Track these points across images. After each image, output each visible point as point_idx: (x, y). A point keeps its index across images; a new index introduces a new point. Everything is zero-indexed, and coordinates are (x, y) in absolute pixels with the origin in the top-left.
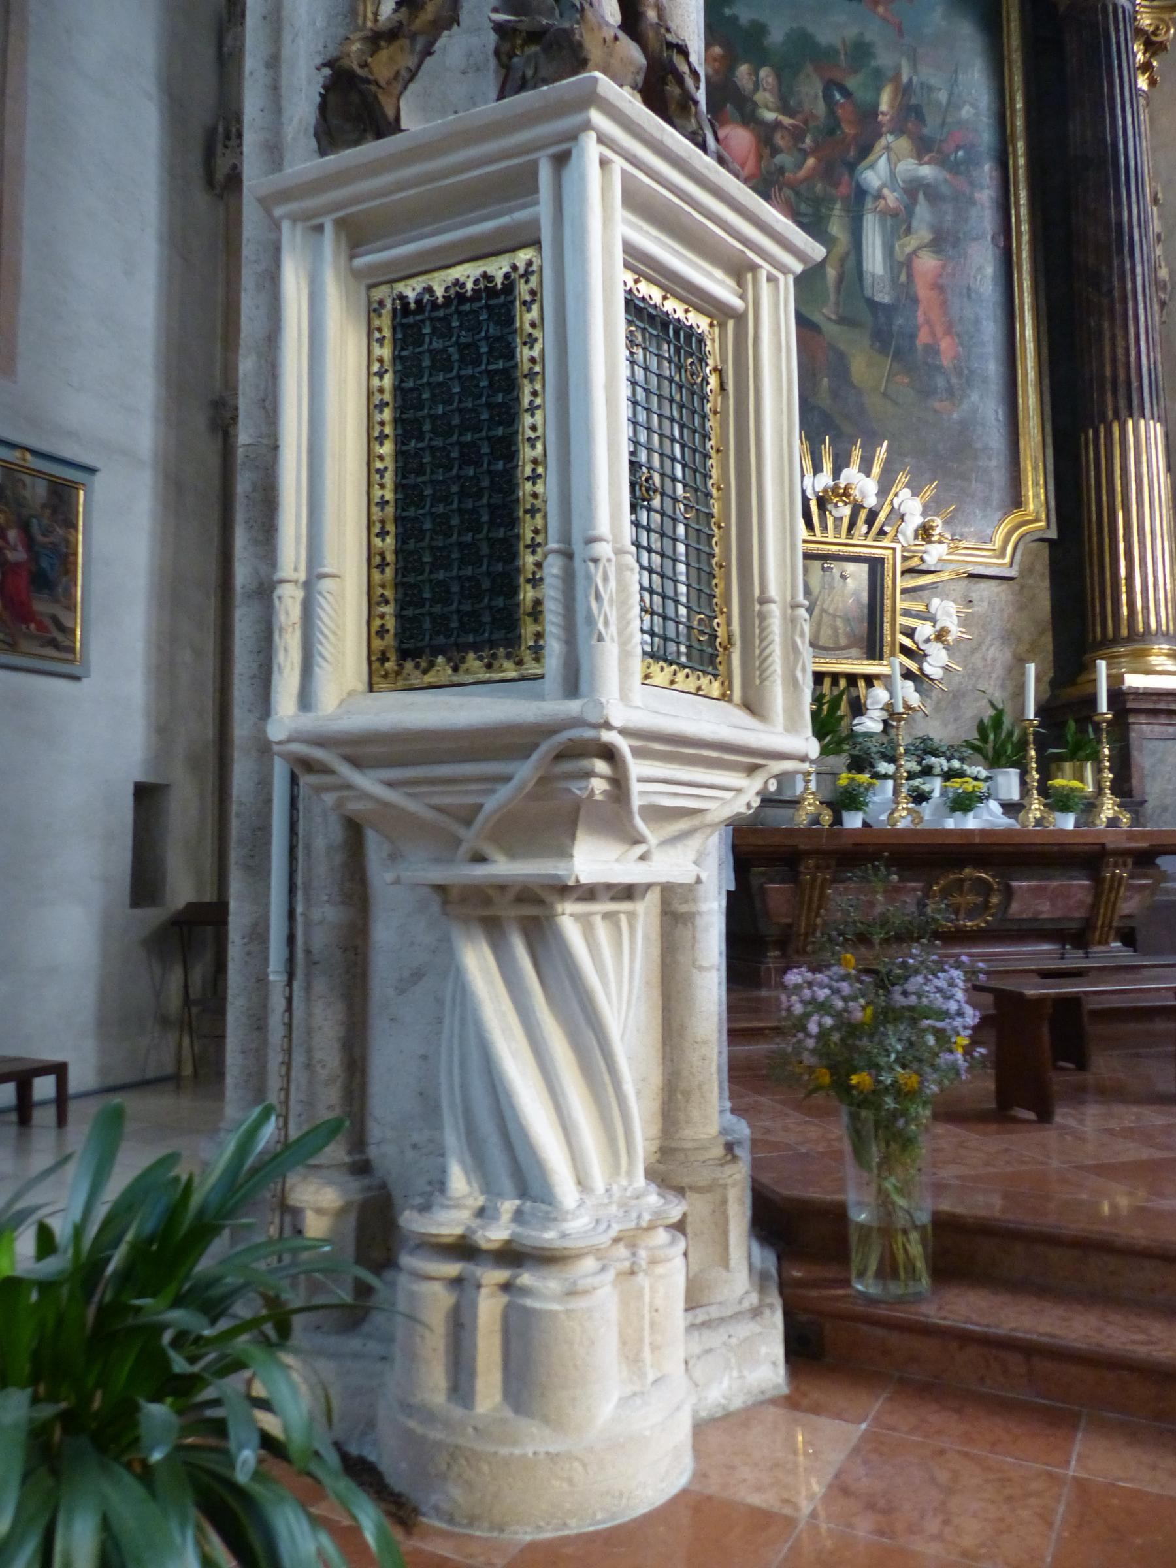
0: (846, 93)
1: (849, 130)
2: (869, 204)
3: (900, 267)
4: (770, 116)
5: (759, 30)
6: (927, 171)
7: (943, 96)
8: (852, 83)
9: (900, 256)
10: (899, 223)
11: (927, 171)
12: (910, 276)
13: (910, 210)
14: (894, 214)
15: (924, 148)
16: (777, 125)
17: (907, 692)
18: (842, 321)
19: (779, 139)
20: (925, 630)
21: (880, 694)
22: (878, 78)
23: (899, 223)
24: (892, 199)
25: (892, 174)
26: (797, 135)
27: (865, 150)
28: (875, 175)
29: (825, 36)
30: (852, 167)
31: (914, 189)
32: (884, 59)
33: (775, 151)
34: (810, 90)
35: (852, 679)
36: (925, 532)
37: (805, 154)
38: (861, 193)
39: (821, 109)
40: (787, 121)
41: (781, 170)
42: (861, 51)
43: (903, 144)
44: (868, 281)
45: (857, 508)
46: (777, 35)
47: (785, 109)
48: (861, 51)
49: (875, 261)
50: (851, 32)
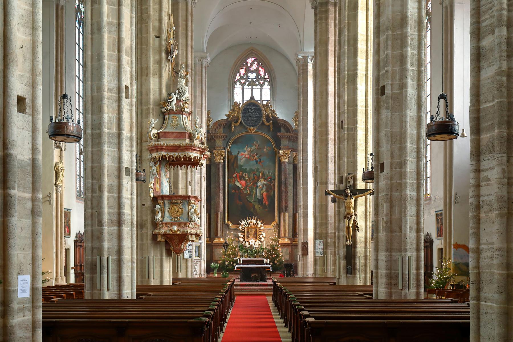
3: (262, 195)
5: (246, 169)
6: (265, 182)
8: (257, 173)
11: (265, 182)
15: (265, 180)
20: (261, 236)
22: (260, 172)
23: (262, 189)
24: (261, 186)
26: (250, 181)
28: (259, 184)
29: (253, 168)
30: (256, 183)
31: (264, 185)
32: (260, 170)
34: (252, 175)
36: (261, 226)
38: (257, 186)
43: (263, 179)
46: (248, 169)
49: (258, 194)
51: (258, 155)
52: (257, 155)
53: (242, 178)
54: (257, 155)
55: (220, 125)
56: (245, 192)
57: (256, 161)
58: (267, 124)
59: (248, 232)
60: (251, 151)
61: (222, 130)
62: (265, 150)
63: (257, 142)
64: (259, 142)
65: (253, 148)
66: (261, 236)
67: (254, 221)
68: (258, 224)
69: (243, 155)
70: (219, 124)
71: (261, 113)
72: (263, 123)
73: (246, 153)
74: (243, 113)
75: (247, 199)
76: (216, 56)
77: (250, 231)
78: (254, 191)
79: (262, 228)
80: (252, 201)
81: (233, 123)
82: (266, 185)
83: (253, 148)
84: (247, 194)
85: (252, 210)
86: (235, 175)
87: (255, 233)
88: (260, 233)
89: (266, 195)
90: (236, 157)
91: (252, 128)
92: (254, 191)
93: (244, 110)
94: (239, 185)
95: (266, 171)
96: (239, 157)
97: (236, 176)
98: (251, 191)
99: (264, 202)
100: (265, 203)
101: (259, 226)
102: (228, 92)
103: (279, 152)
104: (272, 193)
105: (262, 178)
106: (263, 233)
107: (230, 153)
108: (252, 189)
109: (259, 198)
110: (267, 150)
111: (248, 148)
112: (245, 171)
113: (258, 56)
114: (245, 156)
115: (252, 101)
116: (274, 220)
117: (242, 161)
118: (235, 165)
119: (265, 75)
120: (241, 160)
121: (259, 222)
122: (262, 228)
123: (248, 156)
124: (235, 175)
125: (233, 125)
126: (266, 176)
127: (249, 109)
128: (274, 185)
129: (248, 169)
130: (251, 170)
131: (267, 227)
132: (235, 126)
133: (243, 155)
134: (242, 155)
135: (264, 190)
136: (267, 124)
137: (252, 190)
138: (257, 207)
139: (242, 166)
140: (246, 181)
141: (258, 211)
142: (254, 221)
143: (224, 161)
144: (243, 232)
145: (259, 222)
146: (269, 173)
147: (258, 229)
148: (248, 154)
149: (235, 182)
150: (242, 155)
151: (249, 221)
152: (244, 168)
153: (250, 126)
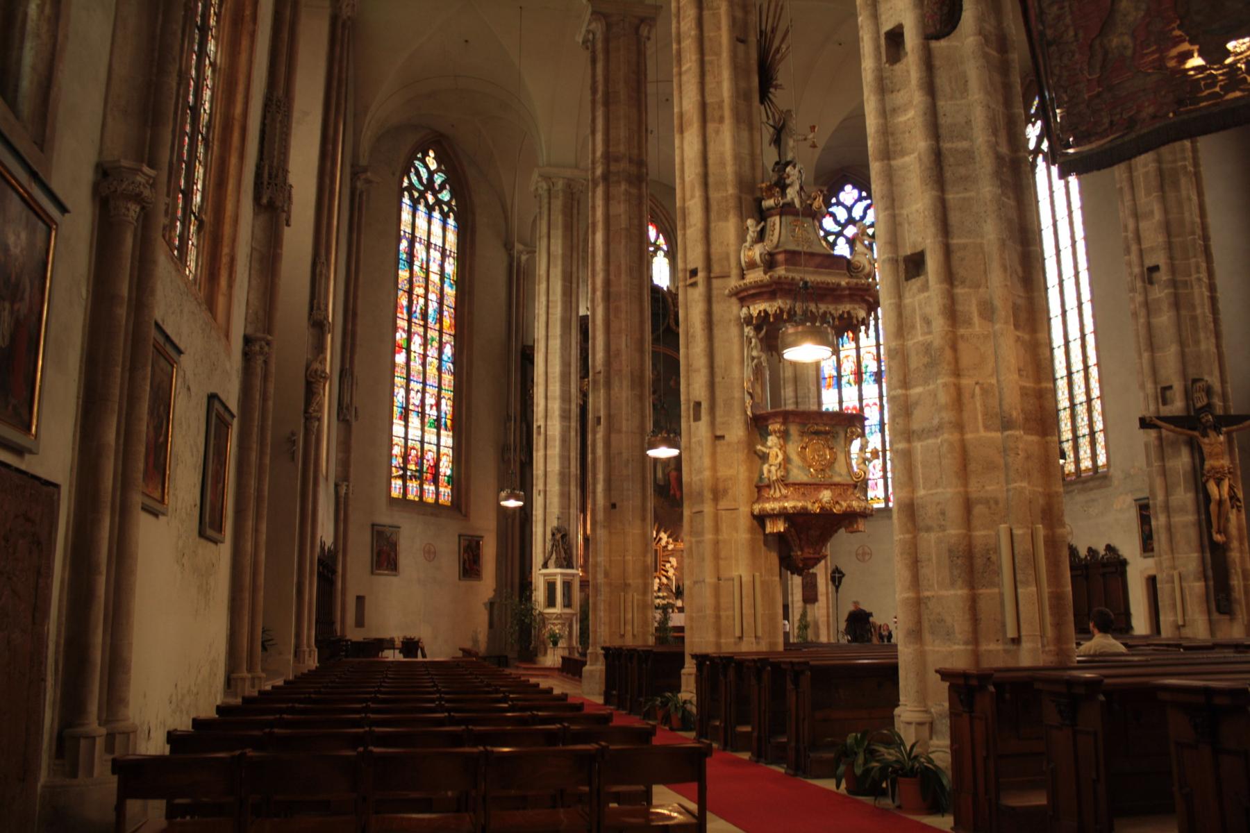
20: (668, 565)
36: (668, 543)
66: (668, 565)
79: (670, 547)
101: (663, 543)
109: (662, 483)
122: (670, 547)
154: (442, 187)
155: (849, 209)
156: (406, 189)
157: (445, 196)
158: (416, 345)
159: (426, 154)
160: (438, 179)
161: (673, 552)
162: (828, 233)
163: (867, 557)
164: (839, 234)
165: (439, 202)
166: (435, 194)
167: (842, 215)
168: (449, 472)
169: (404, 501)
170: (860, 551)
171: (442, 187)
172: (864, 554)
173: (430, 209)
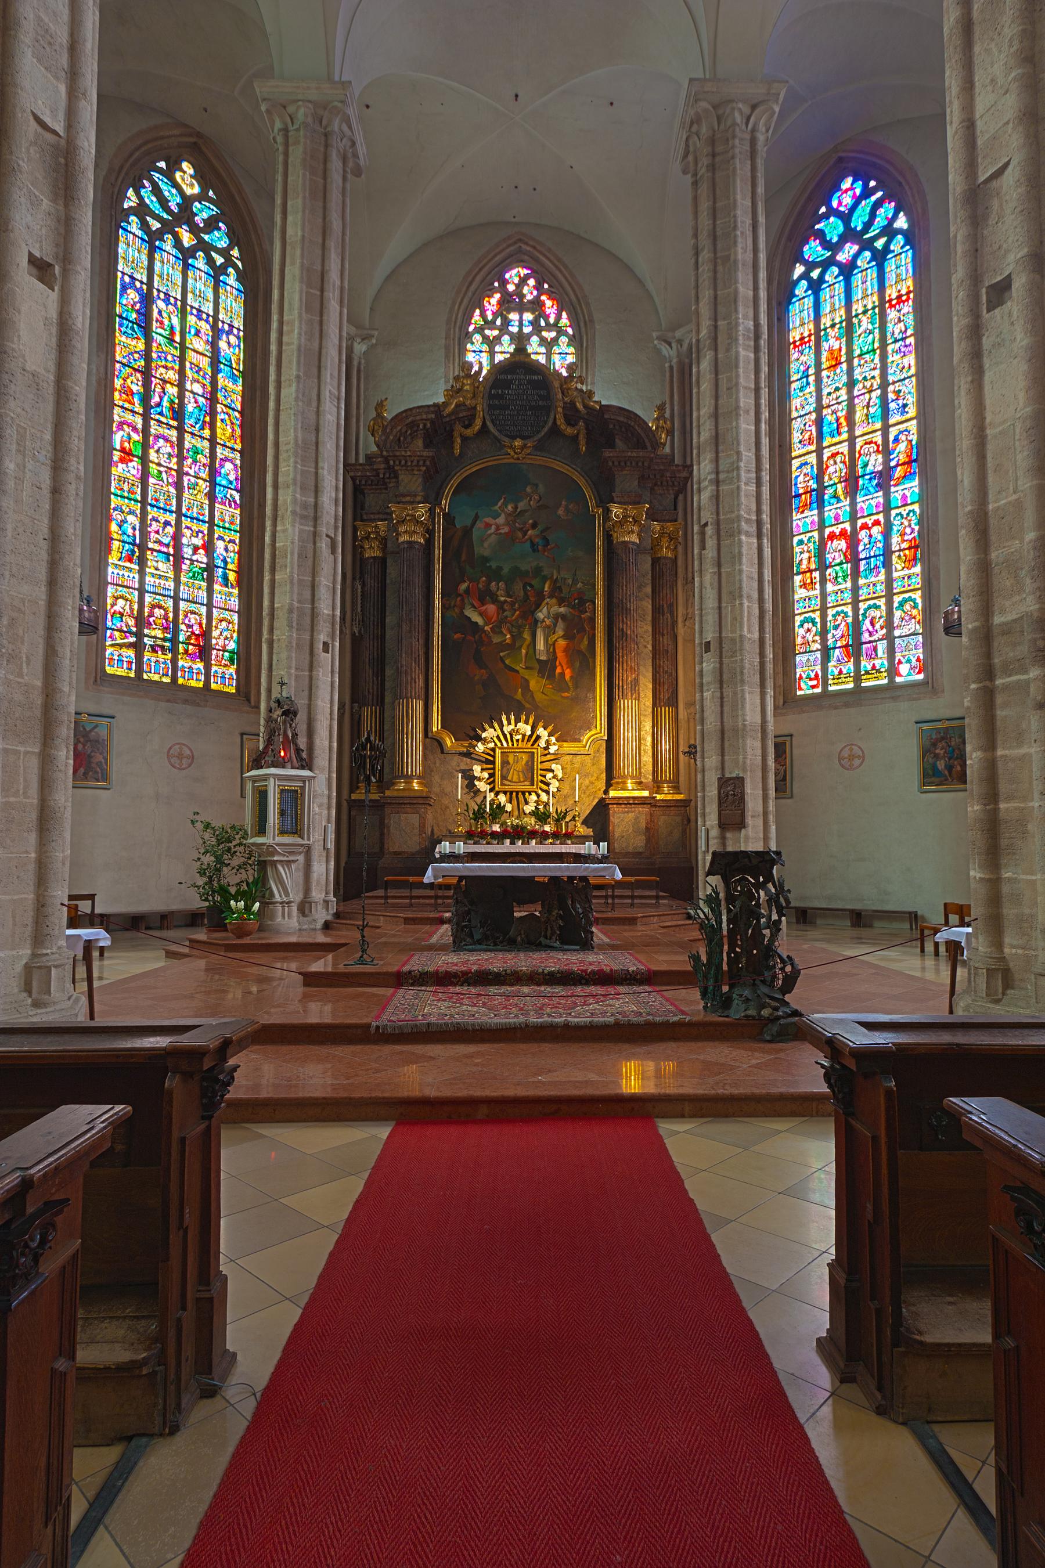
0: (532, 586)
1: (532, 599)
2: (539, 625)
3: (551, 647)
4: (502, 599)
5: (500, 568)
6: (562, 610)
7: (570, 581)
8: (533, 583)
9: (550, 642)
10: (550, 630)
11: (562, 610)
12: (554, 649)
13: (555, 625)
14: (548, 627)
15: (561, 602)
16: (505, 601)
17: (544, 797)
18: (527, 668)
19: (505, 607)
20: (549, 775)
21: (534, 797)
22: (545, 579)
23: (550, 630)
24: (548, 622)
25: (549, 613)
26: (513, 604)
27: (538, 606)
29: (524, 567)
30: (533, 613)
31: (557, 617)
32: (546, 572)
33: (504, 611)
34: (518, 588)
35: (523, 793)
37: (515, 611)
38: (536, 621)
39: (522, 593)
40: (509, 600)
41: (506, 617)
42: (538, 570)
43: (554, 601)
44: (537, 652)
45: (524, 735)
46: (506, 570)
47: (509, 596)
48: (538, 570)
49: (541, 645)
50: (534, 564)
51: (540, 527)
52: (534, 526)
53: (485, 596)
54: (534, 526)
55: (413, 425)
56: (496, 639)
57: (533, 544)
58: (570, 431)
59: (505, 763)
60: (516, 515)
61: (420, 443)
62: (561, 512)
63: (537, 485)
64: (541, 488)
65: (522, 505)
67: (526, 729)
68: (538, 737)
69: (492, 526)
70: (409, 420)
71: (548, 397)
72: (555, 431)
73: (501, 520)
74: (491, 397)
75: (502, 660)
76: (411, 256)
77: (511, 759)
78: (526, 635)
80: (520, 667)
81: (458, 428)
82: (563, 617)
83: (522, 505)
84: (503, 647)
85: (519, 695)
86: (463, 587)
87: (530, 768)
88: (546, 765)
89: (566, 650)
90: (468, 532)
91: (517, 443)
92: (526, 635)
93: (492, 387)
94: (476, 618)
95: (564, 574)
96: (476, 533)
97: (467, 591)
98: (517, 637)
99: (558, 670)
100: (563, 674)
101: (542, 743)
102: (447, 356)
103: (607, 511)
104: (586, 642)
105: (551, 596)
106: (554, 766)
107: (449, 518)
108: (520, 628)
109: (543, 658)
110: (567, 510)
111: (505, 504)
112: (496, 575)
113: (537, 260)
114: (498, 528)
115: (522, 358)
116: (589, 726)
117: (486, 545)
118: (464, 557)
119: (559, 317)
120: (482, 541)
121: (541, 731)
122: (553, 749)
123: (506, 529)
124: (463, 587)
125: (456, 434)
126: (565, 590)
127: (511, 381)
128: (592, 620)
129: (506, 570)
130: (516, 572)
131: (568, 747)
132: (465, 439)
133: (492, 526)
134: (488, 526)
135: (560, 632)
136: (570, 431)
137: (520, 633)
138: (535, 683)
139: (485, 559)
140: (501, 606)
141: (539, 697)
142: (527, 729)
143: (430, 542)
144: (488, 762)
145: (541, 731)
146: (575, 582)
147: (538, 752)
148: (507, 523)
149: (462, 608)
150: (488, 526)
151: (507, 729)
152: (494, 564)
153: (514, 438)
154: (211, 225)
155: (846, 218)
156: (132, 211)
157: (219, 239)
158: (161, 454)
159: (174, 166)
160: (203, 212)
161: (556, 758)
162: (810, 266)
163: (857, 762)
164: (826, 264)
165: (207, 248)
166: (194, 230)
167: (833, 228)
168: (232, 645)
169: (137, 684)
170: (846, 753)
171: (211, 225)
172: (852, 757)
173: (186, 255)
